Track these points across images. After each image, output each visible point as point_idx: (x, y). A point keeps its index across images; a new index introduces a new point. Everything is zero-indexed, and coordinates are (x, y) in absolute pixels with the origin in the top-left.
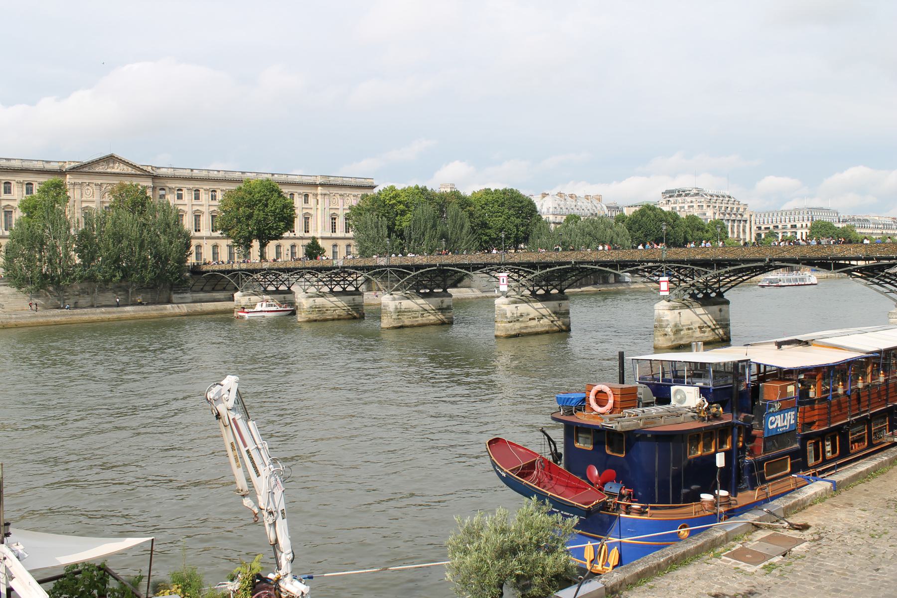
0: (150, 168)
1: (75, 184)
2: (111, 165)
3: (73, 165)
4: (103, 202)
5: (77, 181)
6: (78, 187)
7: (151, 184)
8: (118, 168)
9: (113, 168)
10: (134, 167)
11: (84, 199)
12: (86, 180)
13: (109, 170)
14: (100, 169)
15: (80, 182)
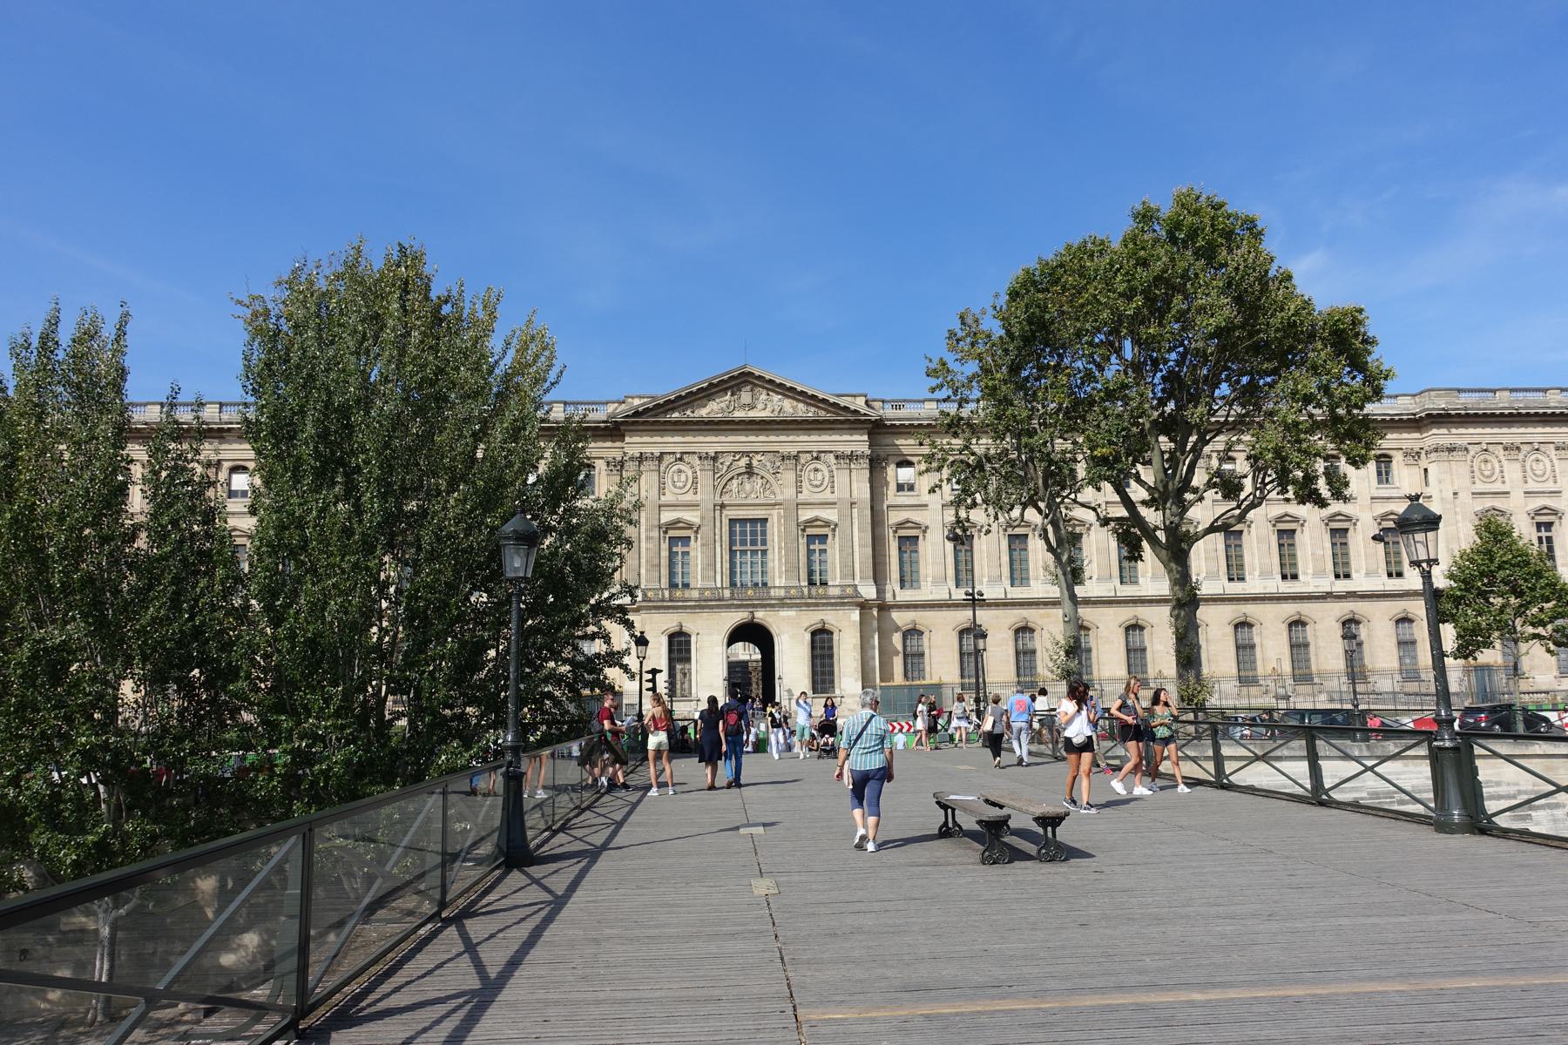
0: (861, 401)
1: (641, 458)
2: (745, 396)
3: (637, 402)
4: (723, 506)
5: (647, 450)
6: (651, 465)
7: (864, 448)
8: (769, 406)
9: (752, 407)
10: (811, 400)
11: (668, 498)
12: (673, 443)
13: (739, 414)
14: (712, 409)
15: (657, 451)
